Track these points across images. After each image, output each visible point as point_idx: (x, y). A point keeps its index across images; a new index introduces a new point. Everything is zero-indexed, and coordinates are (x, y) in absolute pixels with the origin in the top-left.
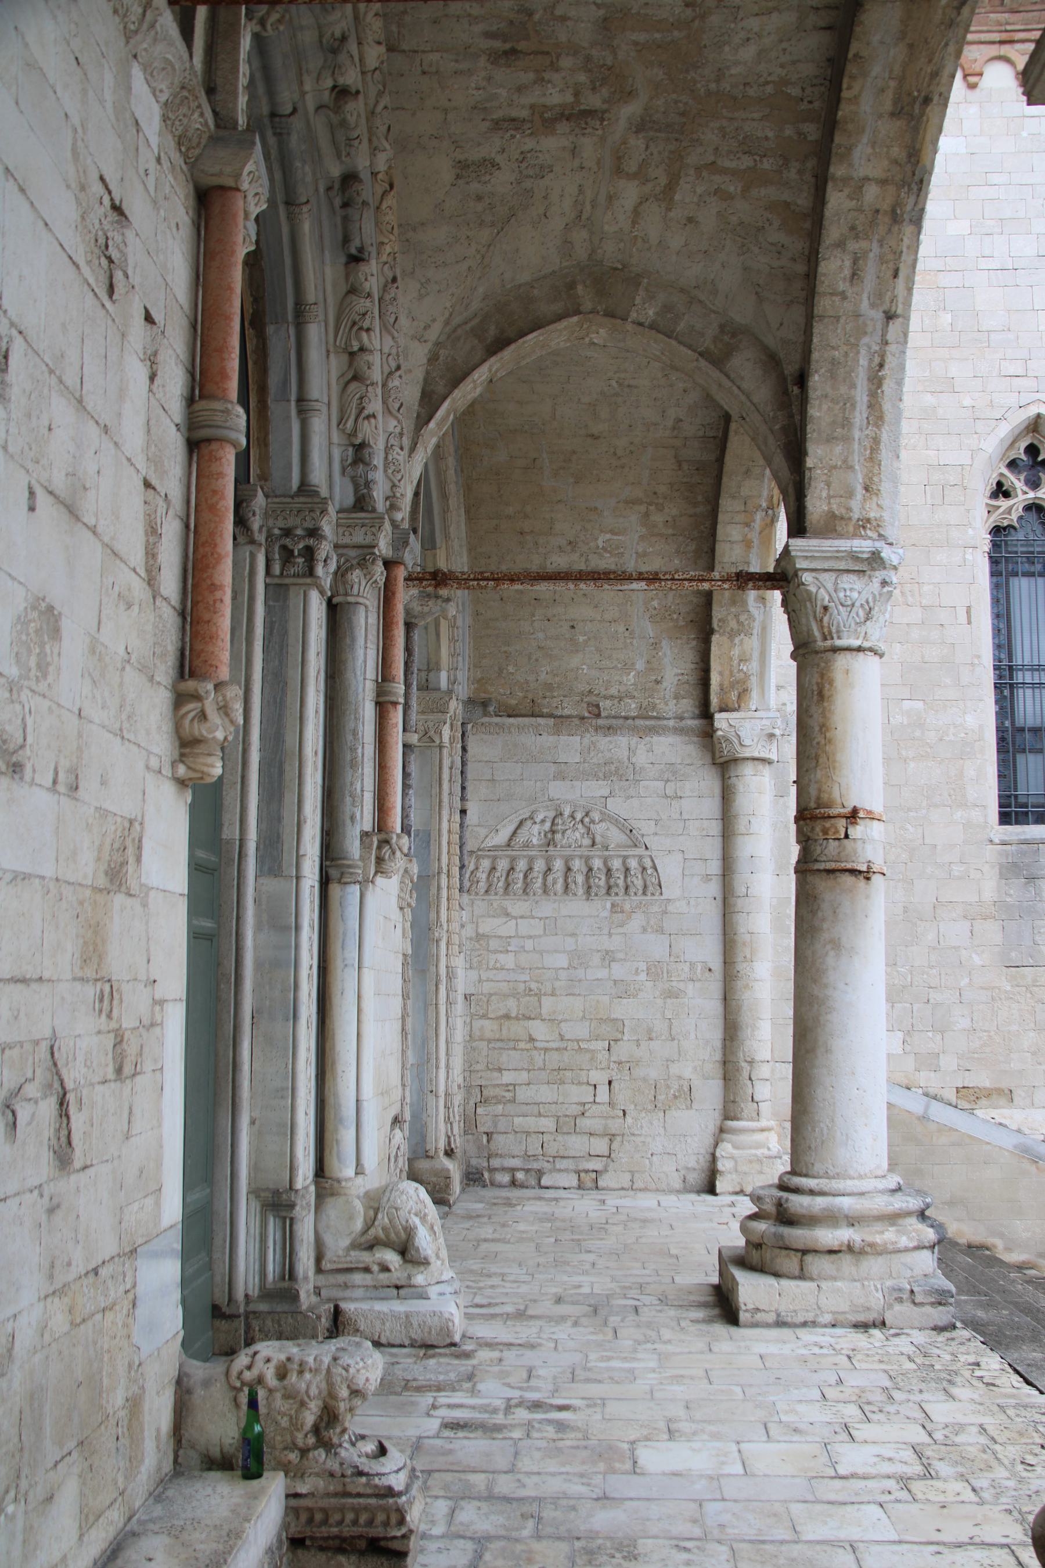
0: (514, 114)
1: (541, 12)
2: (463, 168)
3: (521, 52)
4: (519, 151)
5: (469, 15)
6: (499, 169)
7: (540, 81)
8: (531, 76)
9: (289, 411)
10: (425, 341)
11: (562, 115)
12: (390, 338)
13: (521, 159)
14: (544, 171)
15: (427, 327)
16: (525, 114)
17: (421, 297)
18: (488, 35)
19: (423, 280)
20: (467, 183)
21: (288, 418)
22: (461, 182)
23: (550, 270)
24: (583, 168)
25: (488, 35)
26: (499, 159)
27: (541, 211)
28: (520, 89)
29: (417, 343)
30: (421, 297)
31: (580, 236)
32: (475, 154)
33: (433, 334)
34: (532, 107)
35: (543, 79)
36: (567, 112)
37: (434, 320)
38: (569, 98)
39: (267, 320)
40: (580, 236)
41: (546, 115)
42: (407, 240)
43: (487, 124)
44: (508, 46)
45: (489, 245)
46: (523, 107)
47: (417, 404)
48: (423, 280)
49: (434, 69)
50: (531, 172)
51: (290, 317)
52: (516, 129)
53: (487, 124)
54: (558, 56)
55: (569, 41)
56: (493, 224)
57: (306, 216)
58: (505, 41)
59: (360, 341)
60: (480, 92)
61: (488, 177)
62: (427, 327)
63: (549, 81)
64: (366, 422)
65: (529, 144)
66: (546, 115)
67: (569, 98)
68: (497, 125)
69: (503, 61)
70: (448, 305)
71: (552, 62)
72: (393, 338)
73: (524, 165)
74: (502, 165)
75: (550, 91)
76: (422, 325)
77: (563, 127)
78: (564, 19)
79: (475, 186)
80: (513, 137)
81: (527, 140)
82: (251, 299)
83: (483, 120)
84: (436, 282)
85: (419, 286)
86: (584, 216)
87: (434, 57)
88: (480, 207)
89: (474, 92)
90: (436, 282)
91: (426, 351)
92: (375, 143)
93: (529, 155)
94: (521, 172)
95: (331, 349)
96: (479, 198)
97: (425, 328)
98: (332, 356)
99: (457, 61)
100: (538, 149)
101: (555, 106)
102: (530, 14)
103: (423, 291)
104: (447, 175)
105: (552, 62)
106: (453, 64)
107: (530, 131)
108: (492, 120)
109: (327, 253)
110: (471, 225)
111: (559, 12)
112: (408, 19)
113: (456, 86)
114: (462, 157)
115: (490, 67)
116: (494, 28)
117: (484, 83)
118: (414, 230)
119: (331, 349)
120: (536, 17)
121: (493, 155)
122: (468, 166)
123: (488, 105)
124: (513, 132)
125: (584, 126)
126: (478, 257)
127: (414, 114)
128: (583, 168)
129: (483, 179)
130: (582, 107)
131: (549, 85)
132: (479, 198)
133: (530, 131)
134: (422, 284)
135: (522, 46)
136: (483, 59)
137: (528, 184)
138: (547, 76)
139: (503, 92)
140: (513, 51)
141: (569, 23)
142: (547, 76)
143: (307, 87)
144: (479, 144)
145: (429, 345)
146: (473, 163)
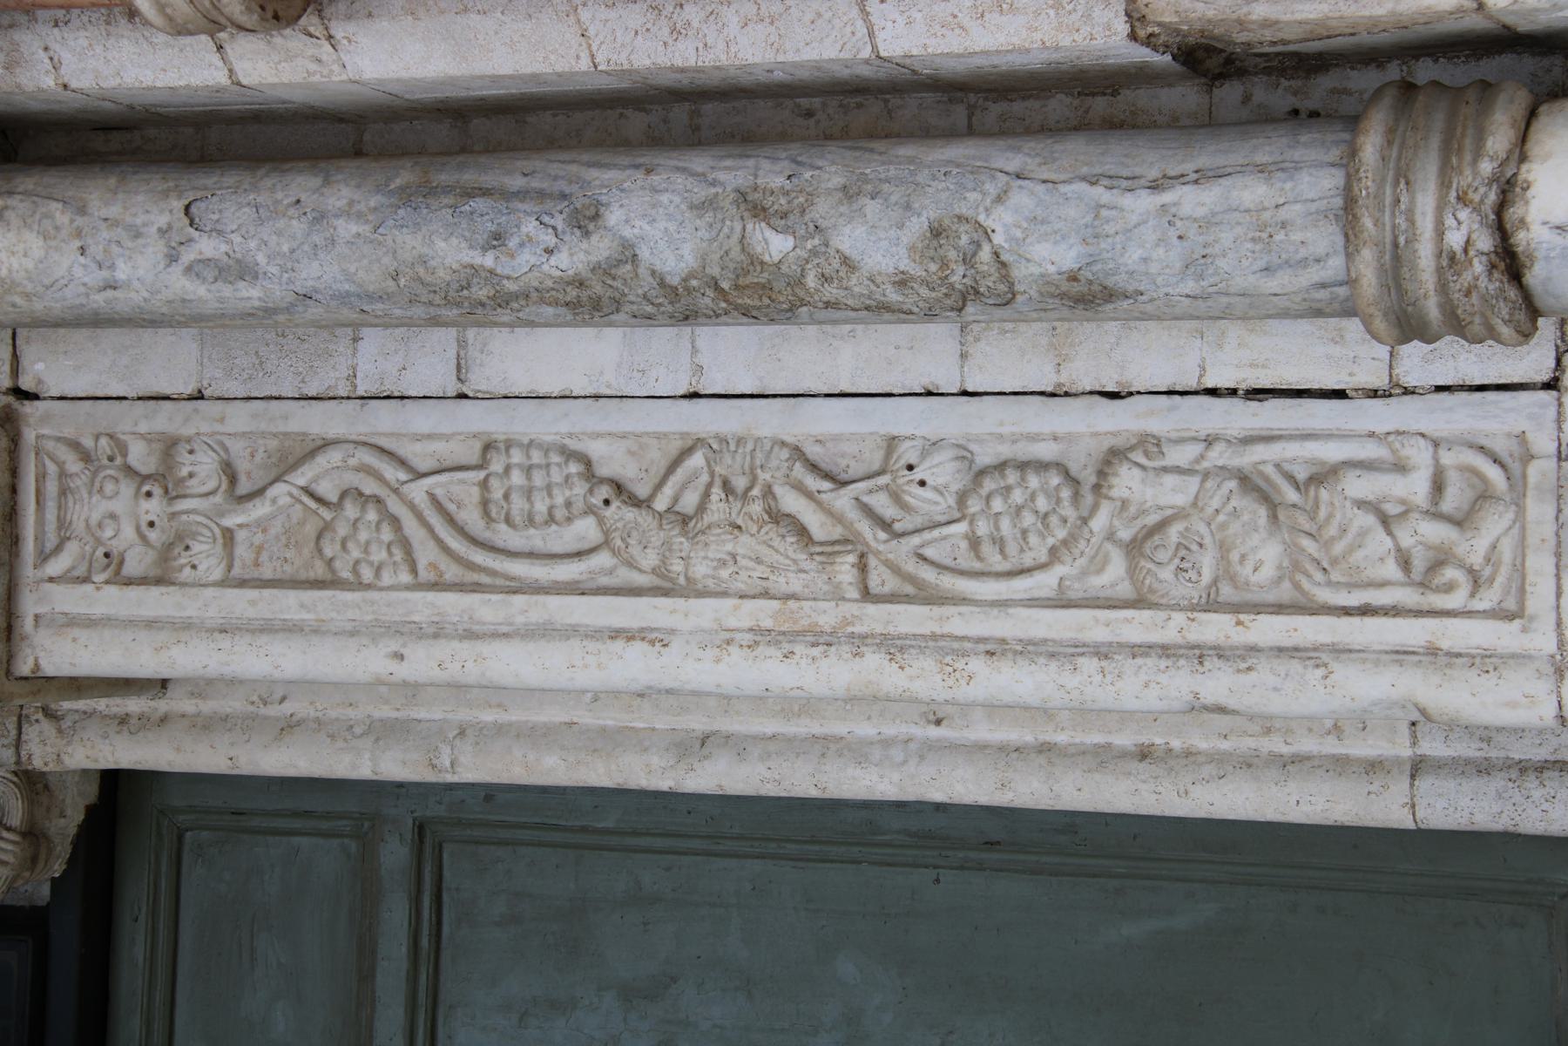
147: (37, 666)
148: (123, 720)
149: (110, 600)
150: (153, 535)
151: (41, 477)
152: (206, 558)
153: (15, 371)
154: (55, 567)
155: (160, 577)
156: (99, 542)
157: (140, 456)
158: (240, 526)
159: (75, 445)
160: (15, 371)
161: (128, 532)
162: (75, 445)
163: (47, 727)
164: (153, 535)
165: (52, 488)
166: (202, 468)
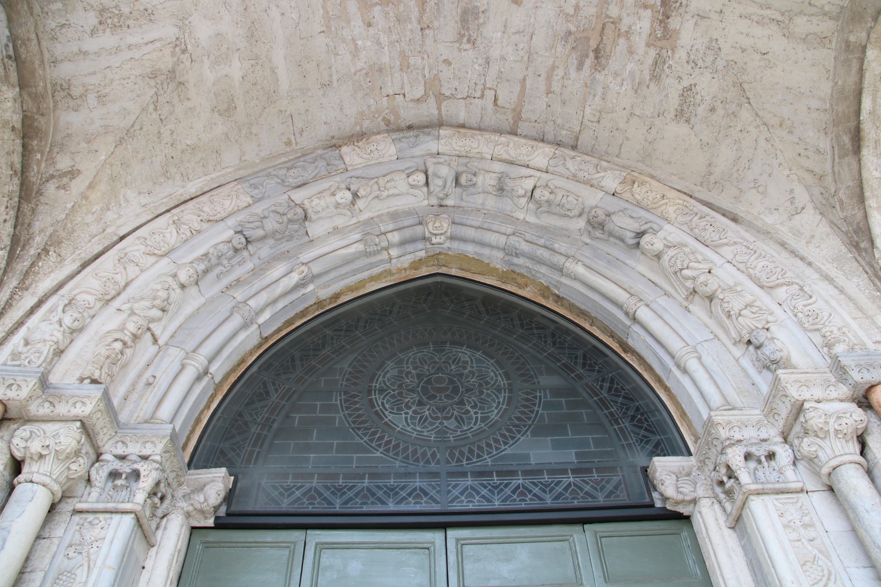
0: (650, 61)
1: (569, 25)
2: (680, 114)
3: (598, 46)
4: (685, 65)
5: (563, 78)
6: (695, 85)
7: (628, 34)
8: (622, 41)
9: (676, 377)
10: (803, 208)
11: (661, 22)
12: (726, 248)
13: (693, 65)
14: (713, 47)
15: (792, 201)
16: (652, 53)
17: (764, 194)
18: (580, 66)
19: (752, 185)
20: (696, 115)
21: (678, 381)
22: (693, 120)
23: (833, 60)
24: (721, 12)
25: (580, 66)
26: (686, 83)
27: (758, 57)
28: (631, 52)
29: (797, 217)
30: (764, 194)
31: (802, 25)
32: (674, 102)
33: (802, 196)
34: (648, 45)
35: (626, 32)
36: (661, 18)
37: (792, 191)
38: (648, 13)
39: (625, 339)
40: (802, 25)
41: (659, 36)
42: (716, 183)
43: (652, 84)
44: (592, 55)
45: (757, 115)
46: (646, 53)
47: (843, 247)
48: (752, 185)
49: (598, 114)
50: (709, 59)
51: (628, 322)
52: (664, 62)
53: (652, 84)
54: (608, 17)
55: (595, 6)
56: (740, 105)
57: (572, 266)
58: (587, 56)
59: (687, 278)
60: (625, 83)
61: (699, 97)
62: (792, 201)
63: (630, 27)
64: (740, 319)
65: (681, 54)
66: (659, 36)
67: (648, 13)
68: (655, 77)
69: (603, 61)
70: (787, 172)
71: (612, 23)
72: (727, 244)
73: (700, 63)
74: (692, 82)
75: (638, 28)
76: (788, 204)
77: (674, 23)
78: (577, 8)
79: (701, 110)
80: (670, 67)
81: (677, 56)
82: (611, 339)
83: (648, 87)
84: (761, 174)
85: (754, 191)
86: (780, 18)
87: (588, 110)
88: (720, 112)
89: (624, 89)
90: (761, 174)
91: (812, 211)
92: (595, 182)
93: (692, 57)
94: (706, 67)
95: (685, 304)
96: (713, 110)
97: (792, 203)
98: (691, 307)
99: (594, 96)
100: (689, 48)
101: (652, 26)
102: (570, 33)
103: (761, 189)
104: (682, 129)
105: (612, 23)
106: (596, 99)
107: (670, 52)
108: (651, 79)
109: (628, 262)
110: (732, 124)
111: (572, 12)
112: (559, 121)
113: (615, 101)
114: (673, 113)
115: (606, 72)
116: (575, 62)
117: (619, 79)
118: (711, 174)
119: (685, 304)
120: (573, 29)
121: (681, 88)
122: (682, 110)
123: (637, 80)
124: (666, 66)
125: (678, 4)
126: (762, 128)
127: (627, 139)
128: (721, 12)
129: (698, 101)
130: (659, 4)
131: (633, 28)
132: (713, 110)
133: (670, 52)
134: (755, 188)
135: (593, 44)
136: (598, 76)
137: (720, 64)
138: (624, 29)
139: (630, 66)
140: (597, 51)
141: (581, 5)
142: (624, 29)
143: (521, 216)
144: (667, 96)
145: (810, 206)
146: (681, 105)
147: (752, 500)
148: (717, 520)
149: (775, 515)
150: (792, 523)
151: (792, 498)
152: (794, 536)
153: (811, 491)
154: (775, 502)
155: (785, 526)
156: (785, 511)
157: (806, 519)
158: (803, 543)
159: (802, 505)
160: (811, 491)
161: (790, 518)
162: (802, 505)
163: (710, 503)
164: (792, 523)
165: (791, 500)
166: (812, 533)
